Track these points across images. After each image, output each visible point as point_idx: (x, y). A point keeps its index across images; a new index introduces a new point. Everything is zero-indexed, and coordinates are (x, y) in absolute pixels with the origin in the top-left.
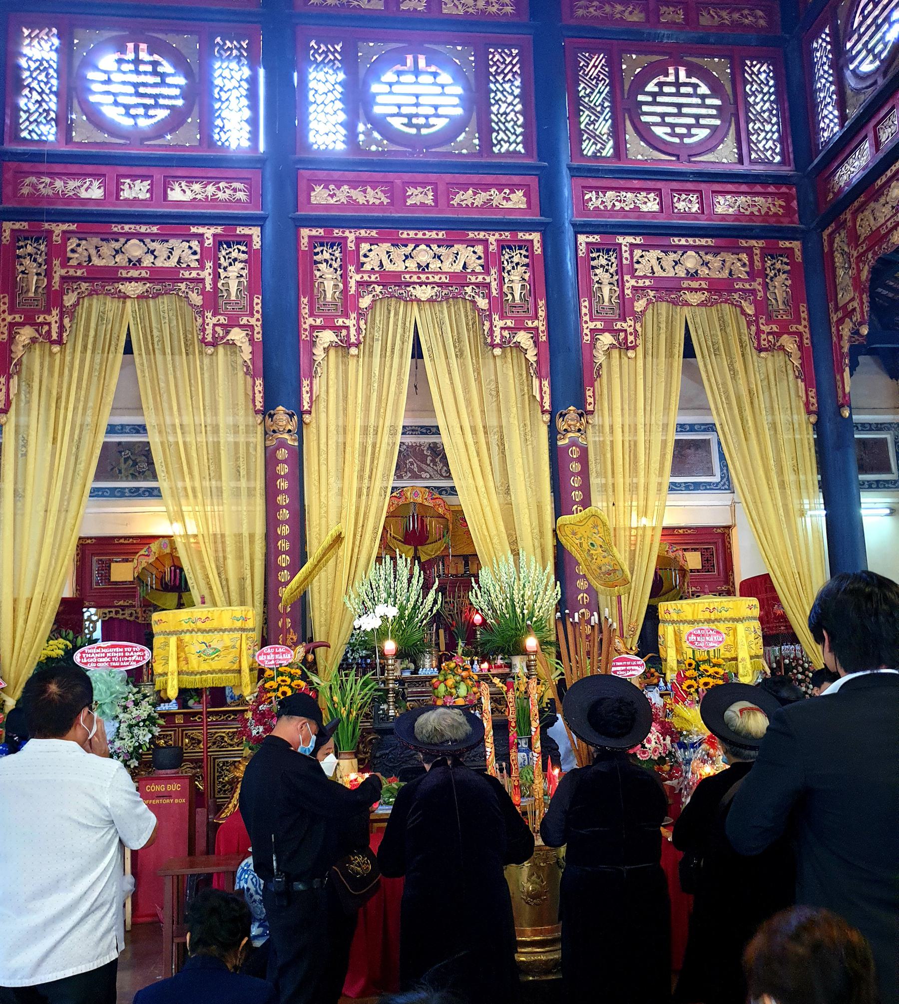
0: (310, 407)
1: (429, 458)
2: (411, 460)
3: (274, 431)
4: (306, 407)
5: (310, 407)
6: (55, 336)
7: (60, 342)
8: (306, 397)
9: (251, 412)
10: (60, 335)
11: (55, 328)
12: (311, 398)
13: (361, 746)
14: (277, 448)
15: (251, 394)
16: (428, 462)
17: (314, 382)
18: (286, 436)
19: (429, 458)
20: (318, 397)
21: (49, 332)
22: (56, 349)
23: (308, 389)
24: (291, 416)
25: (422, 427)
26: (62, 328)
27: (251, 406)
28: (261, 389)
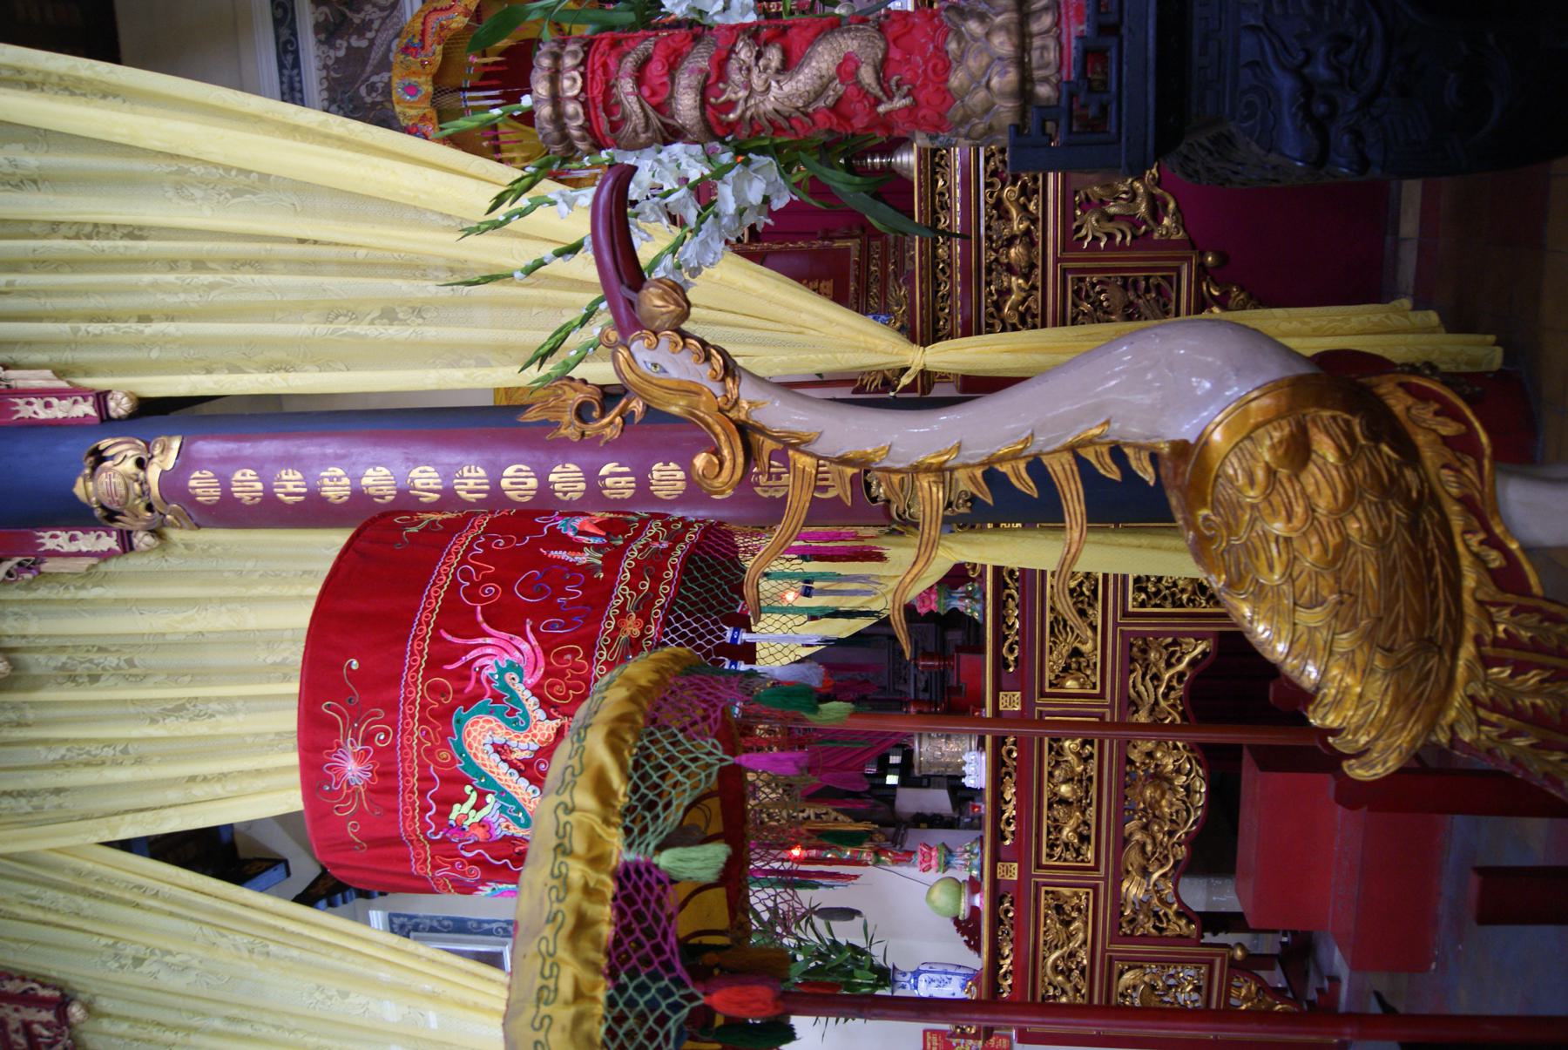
0: (84, 393)
1: (355, 42)
2: (363, 91)
3: (150, 508)
4: (86, 409)
5: (84, 393)
6: (47, 1016)
7: (61, 1004)
8: (61, 410)
9: (132, 562)
10: (43, 1003)
11: (30, 1014)
12: (61, 394)
13: (1113, 210)
14: (189, 500)
15: (84, 563)
16: (364, 44)
17: (21, 384)
18: (153, 474)
19: (355, 42)
20: (59, 373)
21: (47, 1025)
22: (76, 1012)
23: (38, 404)
24: (99, 457)
25: (281, 66)
26: (27, 999)
27: (113, 565)
28: (63, 536)
